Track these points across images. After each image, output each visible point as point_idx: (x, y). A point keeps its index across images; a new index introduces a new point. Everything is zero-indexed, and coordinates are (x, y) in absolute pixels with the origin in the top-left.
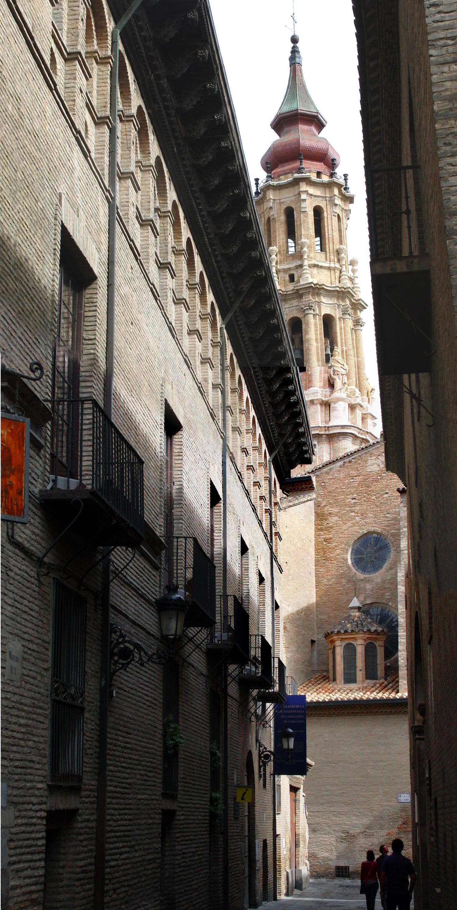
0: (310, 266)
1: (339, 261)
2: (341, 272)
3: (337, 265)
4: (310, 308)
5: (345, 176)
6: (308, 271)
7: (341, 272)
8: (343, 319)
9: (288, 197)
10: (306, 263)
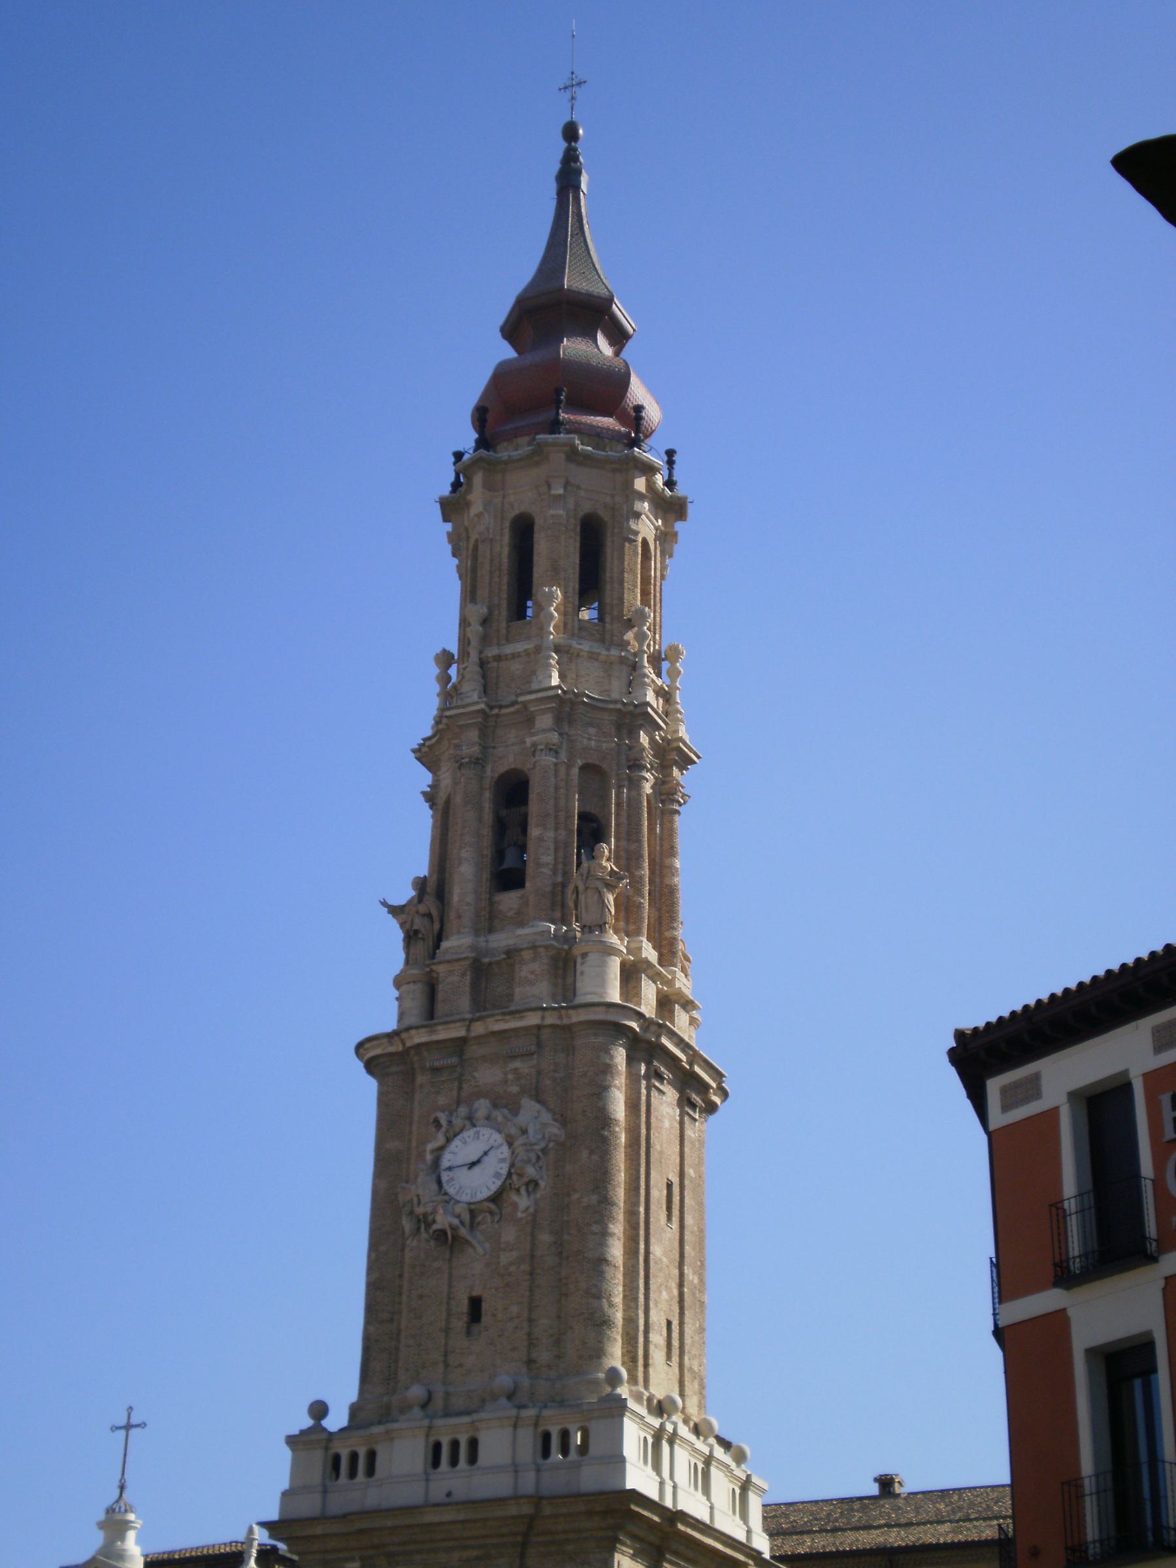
5: (670, 453)
9: (522, 492)
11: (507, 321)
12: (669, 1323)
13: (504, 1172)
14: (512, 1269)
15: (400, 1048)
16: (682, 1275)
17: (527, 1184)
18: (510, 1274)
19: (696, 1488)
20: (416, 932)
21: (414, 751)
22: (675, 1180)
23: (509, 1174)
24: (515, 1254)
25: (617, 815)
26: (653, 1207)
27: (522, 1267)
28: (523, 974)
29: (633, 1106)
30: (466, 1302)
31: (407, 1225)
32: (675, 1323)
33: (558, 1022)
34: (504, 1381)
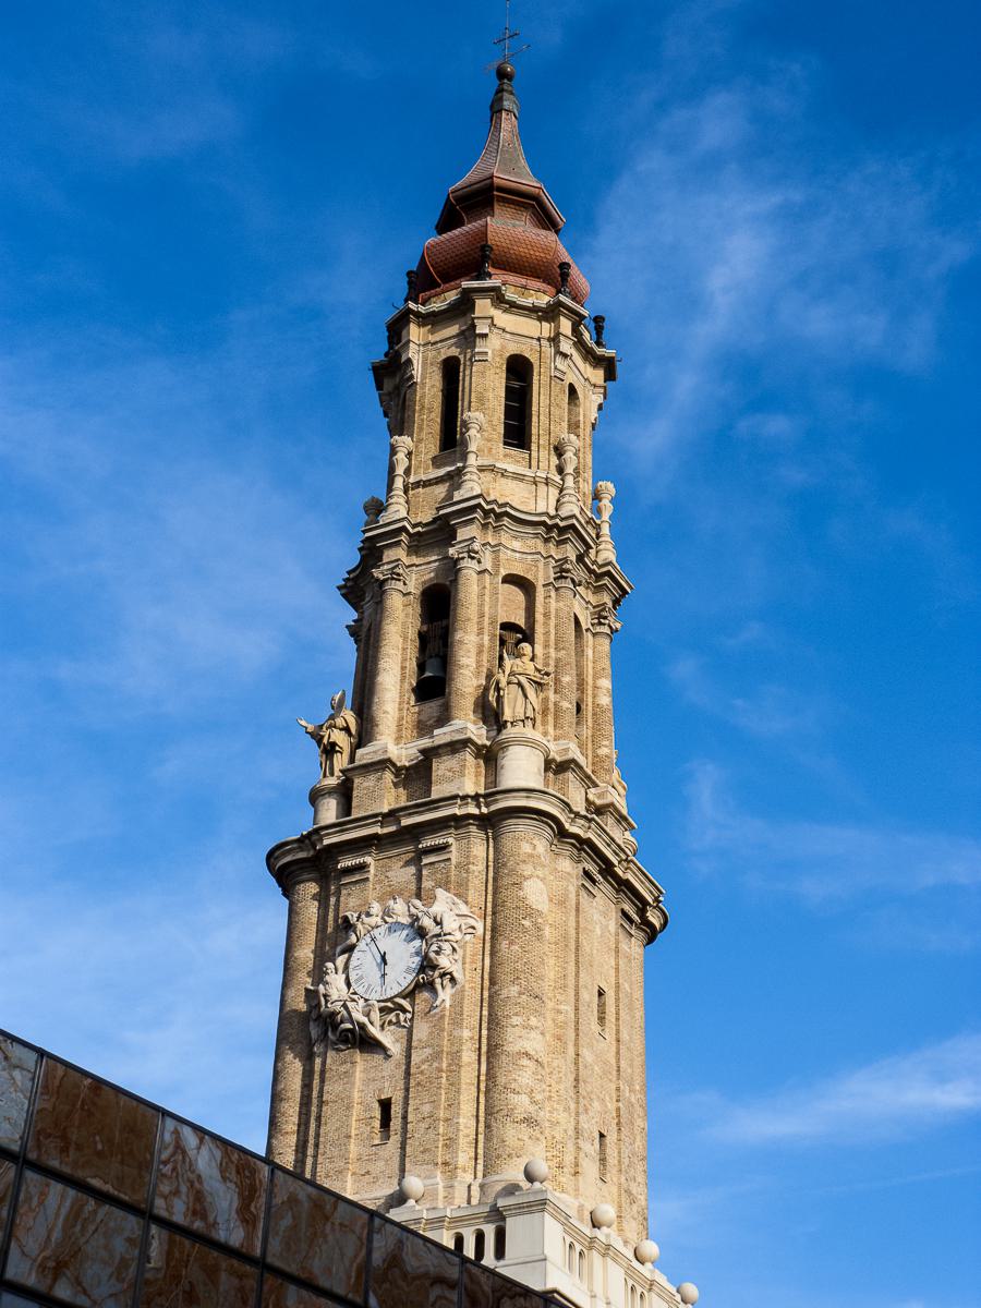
0: (481, 469)
1: (560, 470)
2: (561, 492)
3: (557, 478)
4: (472, 554)
6: (475, 477)
7: (561, 492)
8: (557, 589)
10: (472, 459)
11: (439, 223)
14: (423, 1067)
15: (312, 853)
18: (422, 1072)
19: (438, 509)
20: (334, 744)
21: (339, 588)
24: (428, 1051)
25: (546, 624)
27: (435, 1065)
28: (440, 772)
30: (377, 1105)
31: (314, 1032)
33: (476, 811)
34: (414, 1183)
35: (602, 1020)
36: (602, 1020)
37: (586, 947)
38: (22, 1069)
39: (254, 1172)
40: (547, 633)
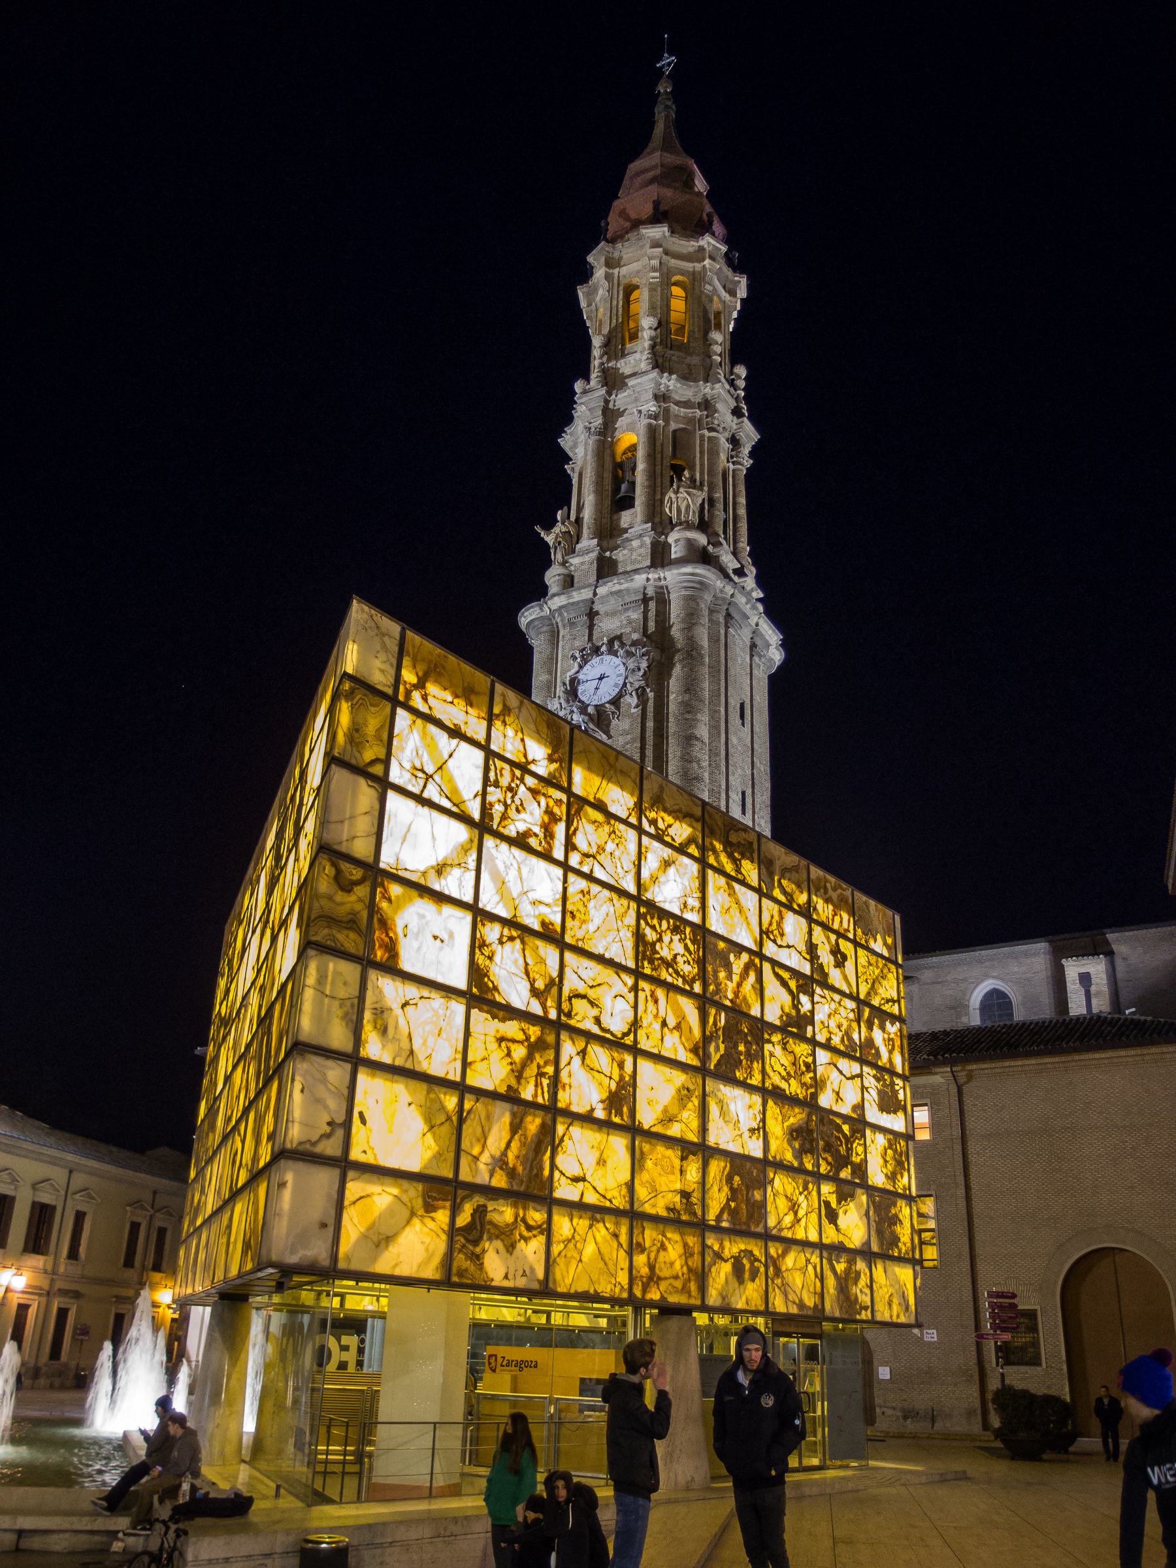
12: (743, 793)
13: (621, 683)
16: (753, 762)
17: (637, 690)
22: (748, 701)
23: (625, 684)
24: (629, 737)
26: (730, 709)
29: (714, 639)
32: (749, 792)
35: (742, 717)
36: (742, 717)
37: (732, 672)
38: (390, 637)
39: (559, 728)
40: (702, 465)
